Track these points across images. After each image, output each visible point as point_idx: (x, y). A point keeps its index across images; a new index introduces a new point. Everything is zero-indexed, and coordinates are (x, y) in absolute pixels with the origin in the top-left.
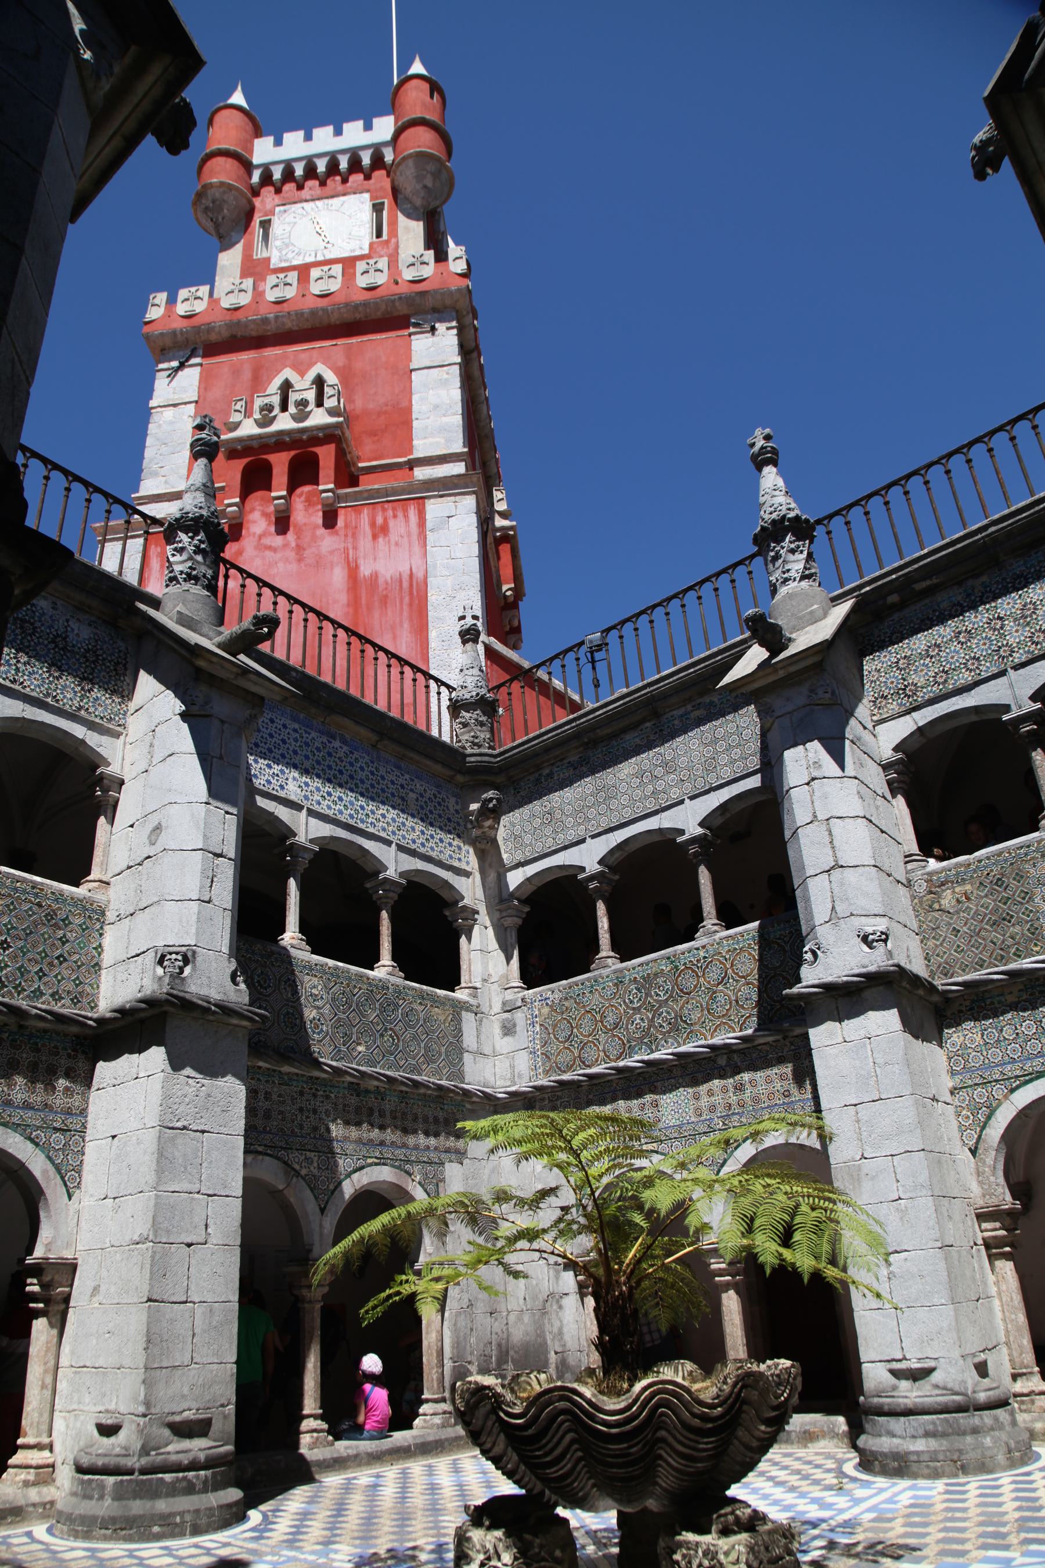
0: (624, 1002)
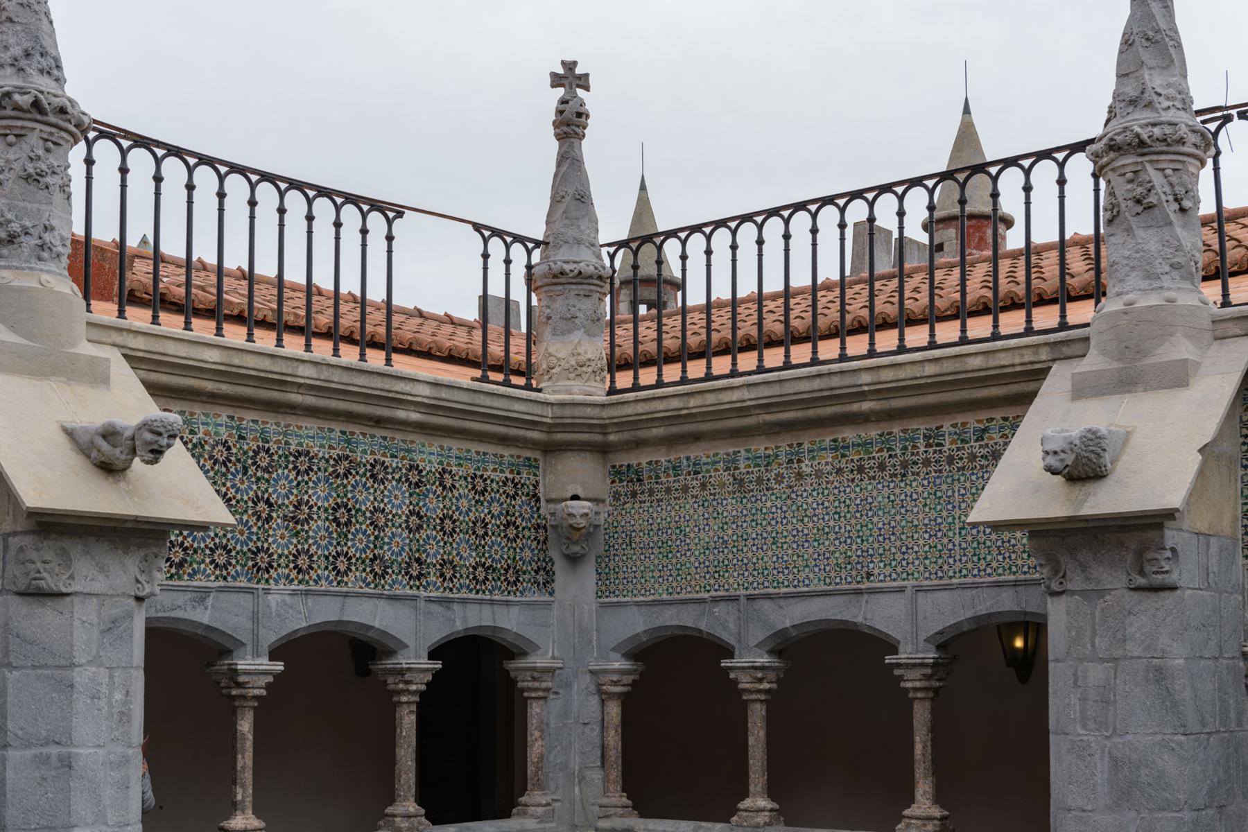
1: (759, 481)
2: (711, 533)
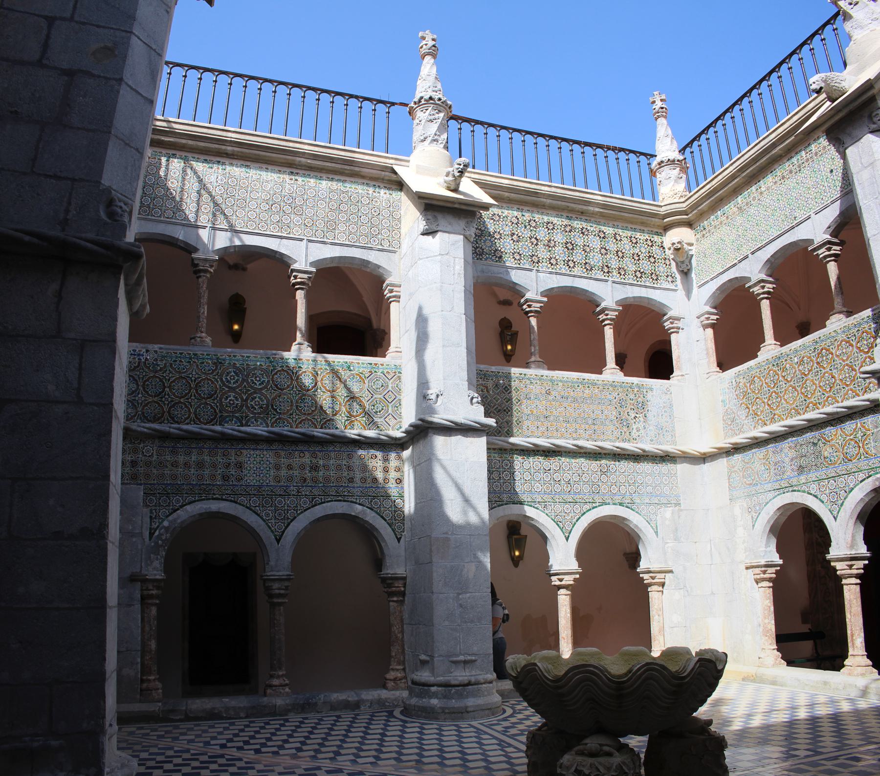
0: (221, 380)
1: (747, 204)
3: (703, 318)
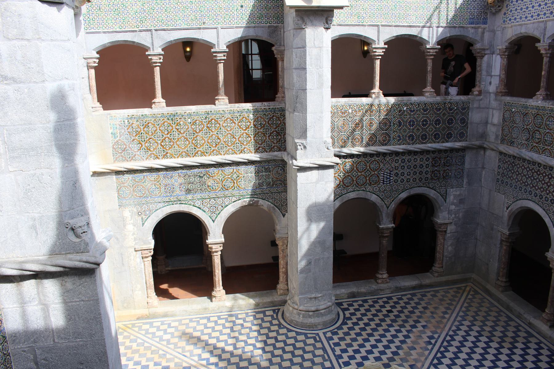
2: (138, 7)
3: (90, 61)
